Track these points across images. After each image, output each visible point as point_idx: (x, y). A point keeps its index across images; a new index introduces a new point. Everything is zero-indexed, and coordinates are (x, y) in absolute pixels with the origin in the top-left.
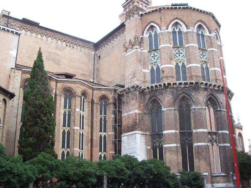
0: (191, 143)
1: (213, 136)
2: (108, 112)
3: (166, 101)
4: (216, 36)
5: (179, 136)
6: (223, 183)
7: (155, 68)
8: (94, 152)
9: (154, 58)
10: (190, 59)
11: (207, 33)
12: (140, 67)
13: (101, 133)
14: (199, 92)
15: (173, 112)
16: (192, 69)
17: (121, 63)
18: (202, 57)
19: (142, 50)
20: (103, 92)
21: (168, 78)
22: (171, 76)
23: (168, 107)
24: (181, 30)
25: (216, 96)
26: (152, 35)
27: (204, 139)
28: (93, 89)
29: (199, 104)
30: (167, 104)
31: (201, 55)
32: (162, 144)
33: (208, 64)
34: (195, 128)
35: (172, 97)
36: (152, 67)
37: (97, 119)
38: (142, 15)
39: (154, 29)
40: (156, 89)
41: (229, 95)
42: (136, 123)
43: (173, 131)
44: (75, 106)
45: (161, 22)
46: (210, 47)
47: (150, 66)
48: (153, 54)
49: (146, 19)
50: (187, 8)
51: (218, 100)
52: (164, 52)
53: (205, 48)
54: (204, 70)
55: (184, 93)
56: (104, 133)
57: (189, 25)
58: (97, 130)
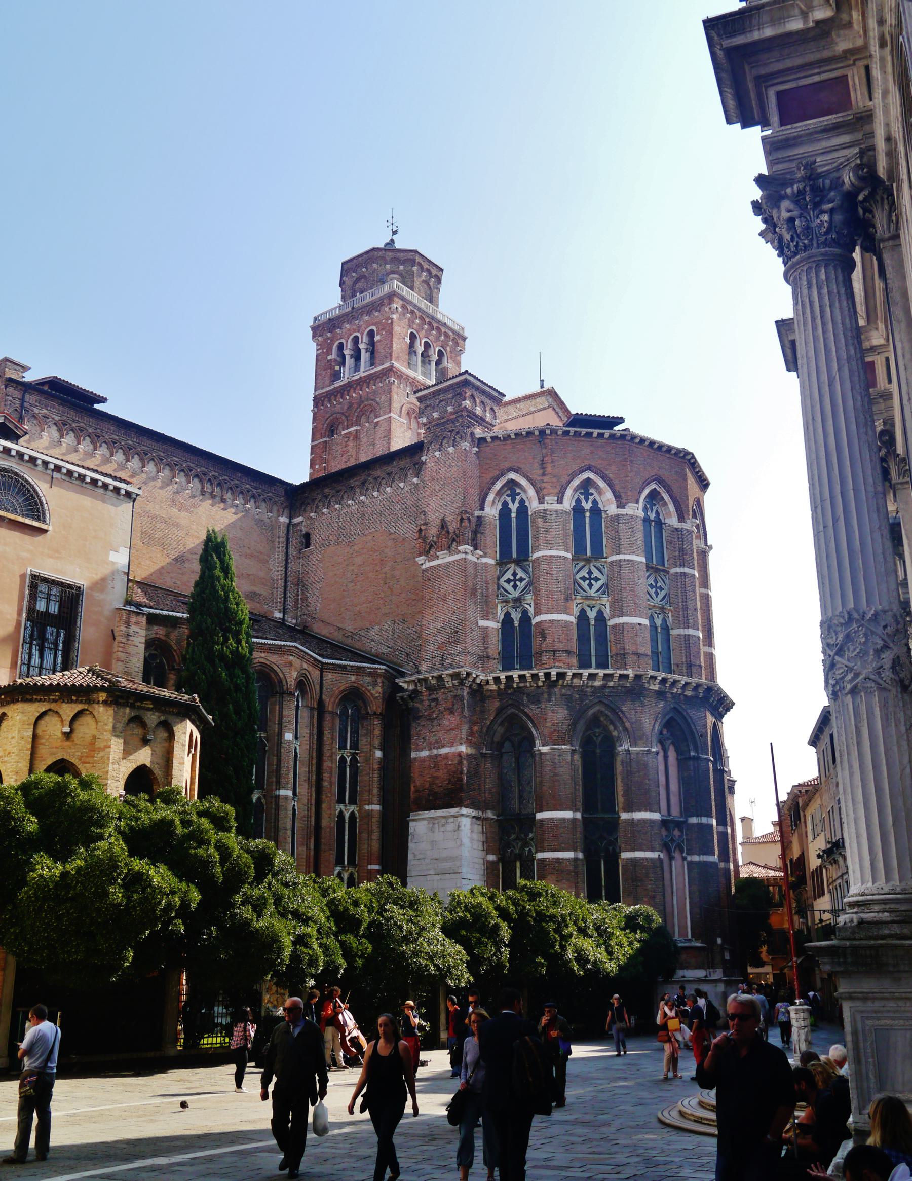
0: (614, 850)
2: (363, 741)
3: (549, 724)
4: (697, 526)
5: (580, 828)
6: (696, 968)
7: (516, 616)
8: (322, 866)
9: (515, 587)
11: (673, 521)
12: (472, 612)
13: (342, 806)
14: (643, 705)
15: (569, 758)
16: (625, 632)
17: (393, 576)
19: (478, 558)
20: (353, 678)
21: (557, 654)
22: (566, 651)
23: (554, 744)
24: (600, 506)
25: (687, 713)
26: (510, 510)
27: (651, 842)
28: (323, 668)
29: (641, 738)
31: (651, 586)
33: (670, 615)
34: (629, 808)
35: (566, 712)
36: (507, 615)
37: (332, 762)
38: (482, 440)
40: (522, 685)
41: (721, 709)
43: (568, 814)
44: (280, 724)
46: (678, 564)
47: (499, 608)
48: (510, 572)
50: (623, 437)
51: (693, 728)
52: (547, 573)
53: (664, 566)
55: (600, 702)
56: (352, 808)
57: (626, 493)
58: (333, 798)
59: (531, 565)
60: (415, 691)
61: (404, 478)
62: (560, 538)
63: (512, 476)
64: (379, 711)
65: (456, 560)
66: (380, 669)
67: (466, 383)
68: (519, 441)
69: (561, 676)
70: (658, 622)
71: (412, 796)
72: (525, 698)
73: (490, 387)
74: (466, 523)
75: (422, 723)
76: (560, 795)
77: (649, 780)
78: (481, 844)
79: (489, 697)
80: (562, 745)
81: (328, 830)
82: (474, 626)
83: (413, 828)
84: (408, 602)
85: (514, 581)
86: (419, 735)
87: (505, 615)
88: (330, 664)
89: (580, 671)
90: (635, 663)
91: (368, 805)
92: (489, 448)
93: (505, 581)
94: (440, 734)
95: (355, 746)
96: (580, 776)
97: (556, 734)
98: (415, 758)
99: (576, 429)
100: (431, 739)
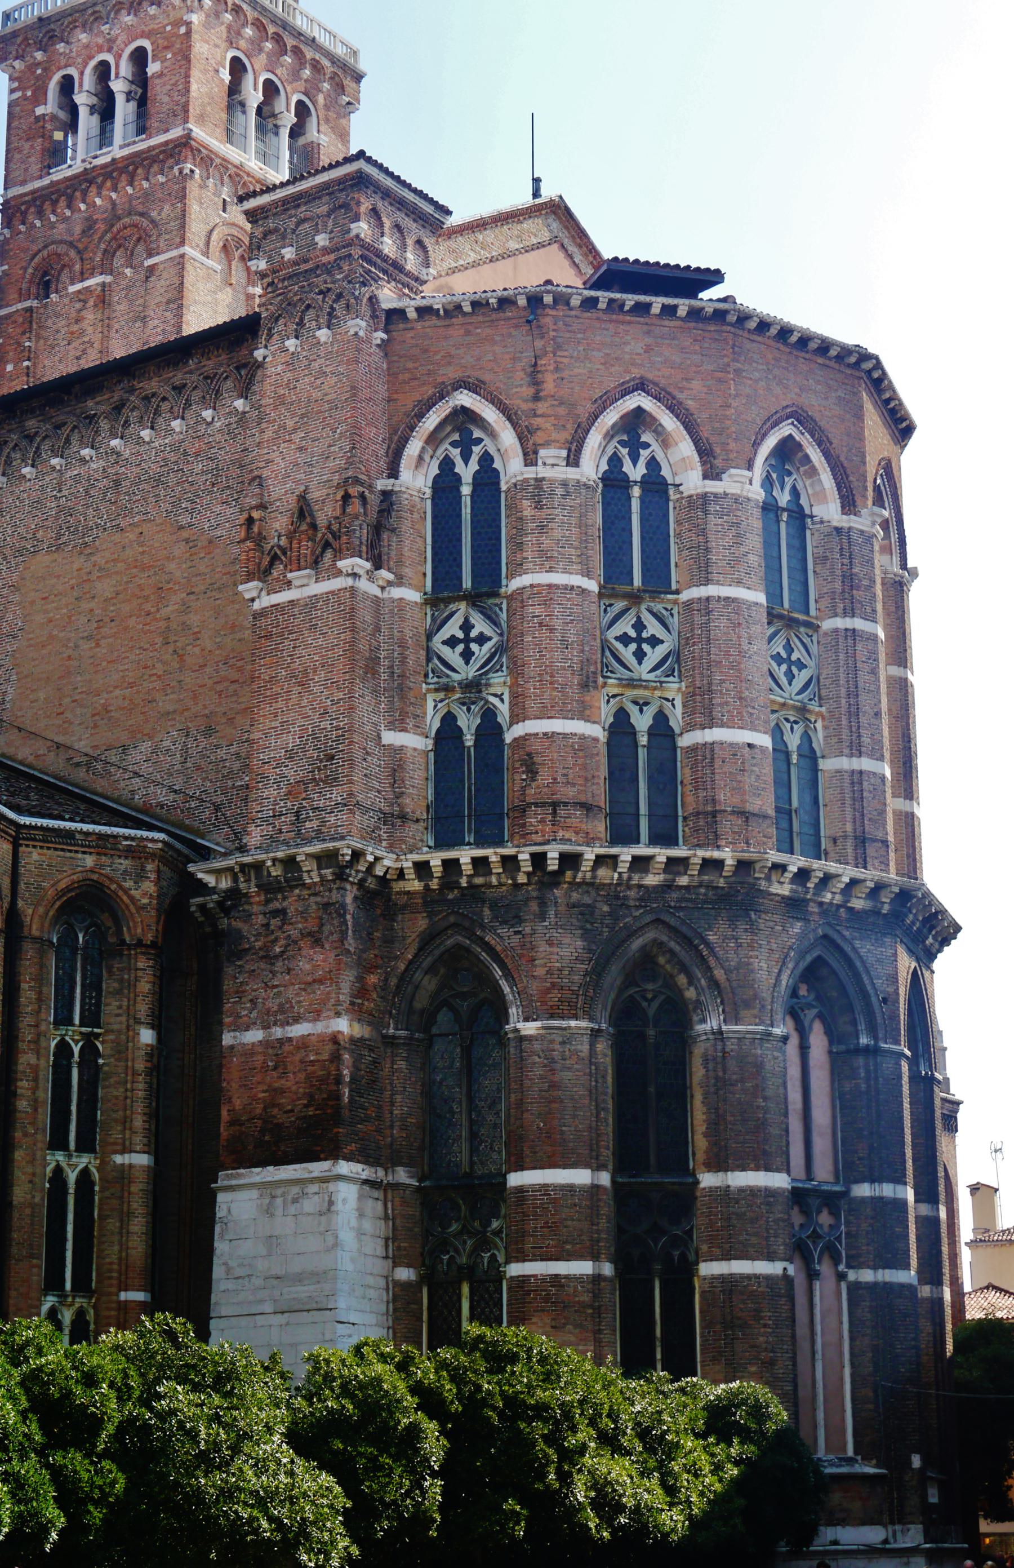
0: (683, 1256)
1: (819, 1212)
2: (111, 1007)
3: (540, 972)
4: (885, 525)
5: (607, 1208)
6: (863, 1523)
7: (468, 723)
8: (13, 1293)
9: (467, 656)
10: (710, 691)
13: (60, 1156)
14: (753, 929)
15: (586, 1048)
16: (718, 763)
17: (185, 626)
18: (780, 671)
19: (383, 588)
20: (89, 861)
21: (562, 812)
23: (552, 1017)
24: (665, 472)
25: (854, 949)
26: (458, 479)
27: (767, 1238)
29: (748, 1005)
30: (548, 991)
31: (778, 658)
32: (493, 1256)
33: (819, 725)
34: (719, 1163)
35: (580, 943)
36: (449, 720)
37: (38, 1053)
38: (396, 315)
39: (477, 434)
40: (479, 881)
41: (930, 940)
42: (338, 1109)
43: (580, 1177)
45: (536, 398)
46: (840, 611)
47: (430, 704)
48: (457, 620)
49: (426, 351)
50: (719, 315)
52: (541, 624)
53: (807, 613)
54: (789, 763)
55: (658, 921)
56: (83, 1160)
58: (39, 1137)
59: (504, 606)
60: (234, 894)
61: (214, 398)
62: (571, 546)
63: (465, 399)
64: (149, 937)
65: (332, 592)
66: (153, 840)
67: (360, 180)
68: (481, 318)
69: (570, 860)
70: (793, 741)
71: (224, 1132)
72: (487, 912)
73: (415, 191)
74: (355, 507)
75: (248, 967)
76: (562, 1133)
77: (765, 1099)
78: (381, 1242)
79: (404, 907)
80: (570, 1018)
81: (28, 1211)
82: (371, 745)
83: (224, 1207)
84: (219, 688)
85: (465, 642)
86: (240, 993)
87: (443, 720)
88: (36, 828)
89: (614, 851)
90: (739, 834)
91: (122, 1152)
92: (411, 334)
93: (444, 643)
94: (291, 992)
95: (92, 1017)
96: (610, 1090)
97: (555, 996)
98: (232, 1047)
99: (612, 295)
100: (269, 1004)
